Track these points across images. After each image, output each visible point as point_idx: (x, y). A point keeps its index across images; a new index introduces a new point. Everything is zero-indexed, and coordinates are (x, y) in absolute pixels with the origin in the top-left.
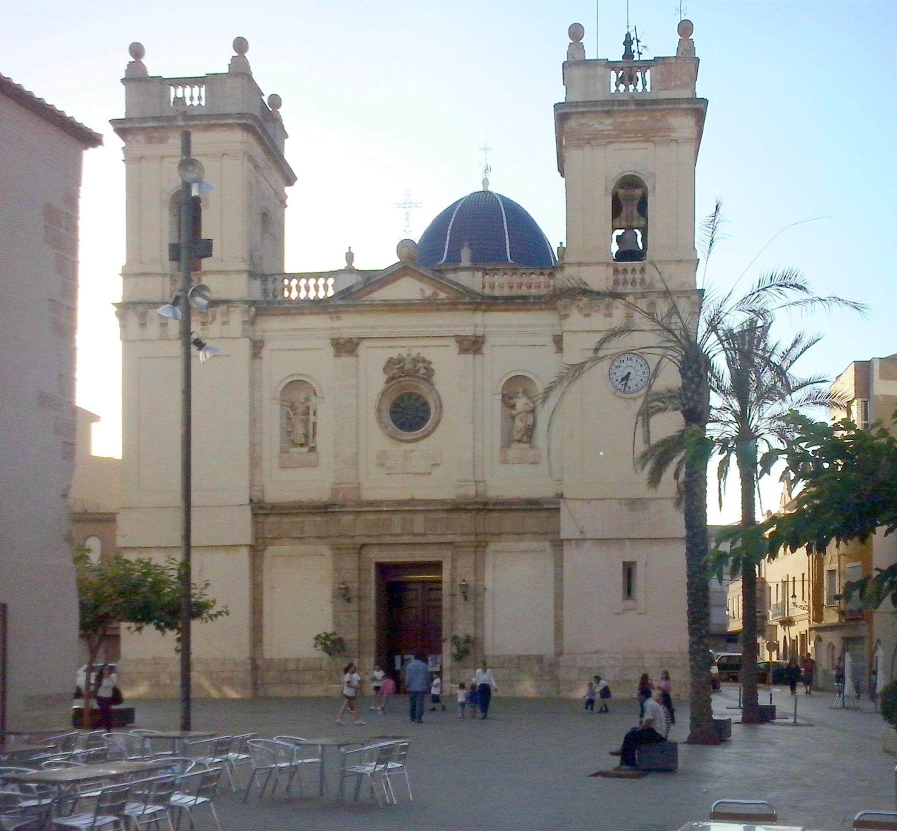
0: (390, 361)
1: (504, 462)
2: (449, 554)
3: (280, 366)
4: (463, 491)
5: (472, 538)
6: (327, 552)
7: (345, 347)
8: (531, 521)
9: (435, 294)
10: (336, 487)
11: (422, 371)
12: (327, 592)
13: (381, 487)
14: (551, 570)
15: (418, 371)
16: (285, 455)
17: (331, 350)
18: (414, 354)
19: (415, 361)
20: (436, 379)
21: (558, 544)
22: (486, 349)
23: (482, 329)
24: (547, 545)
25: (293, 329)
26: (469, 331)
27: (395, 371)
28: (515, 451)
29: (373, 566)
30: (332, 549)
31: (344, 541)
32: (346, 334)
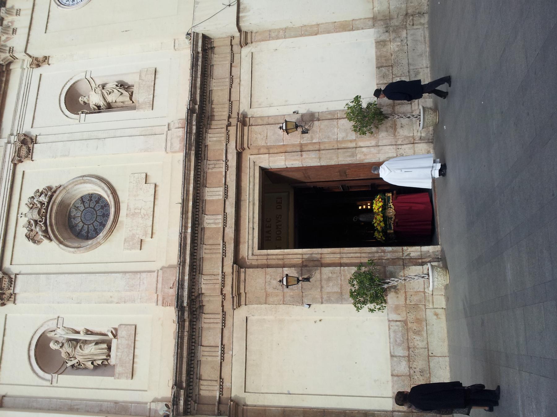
2: (252, 157)
5: (232, 130)
6: (241, 313)
10: (160, 302)
11: (43, 199)
12: (299, 312)
14: (273, 44)
15: (42, 204)
18: (24, 209)
20: (54, 185)
21: (245, 38)
23: (12, 137)
24: (246, 51)
27: (38, 229)
28: (140, 96)
29: (265, 252)
30: (239, 305)
31: (228, 289)
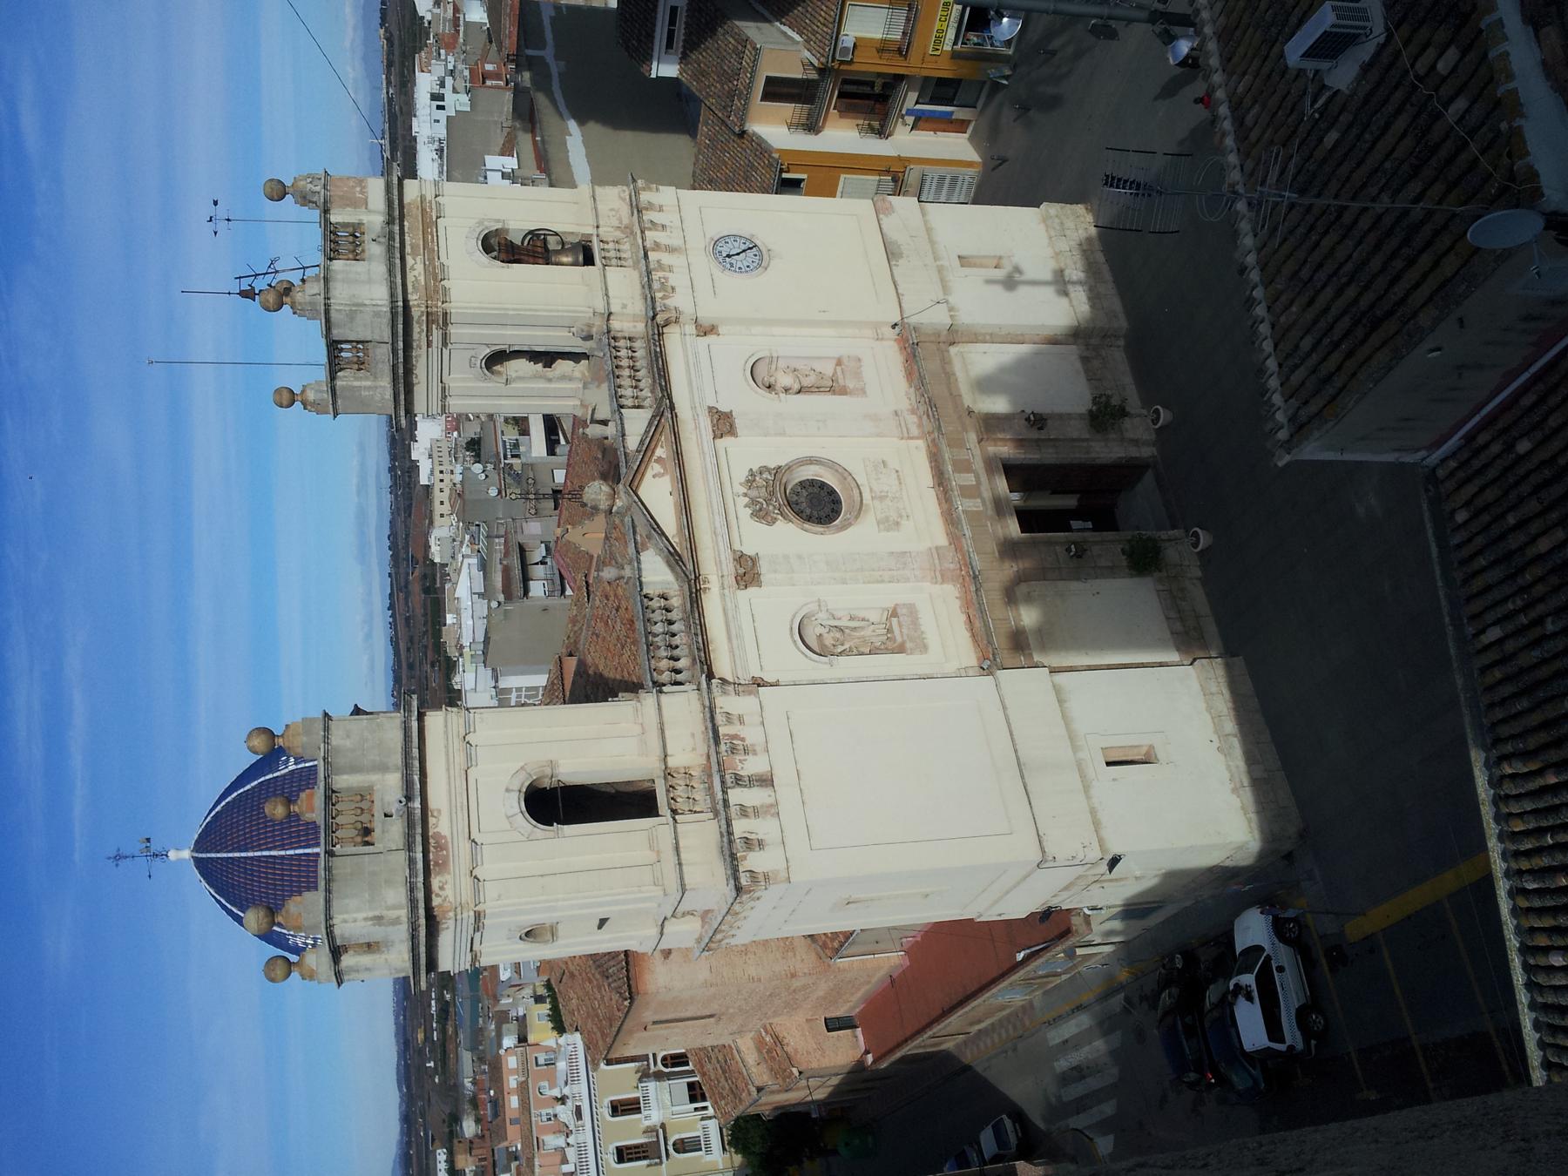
0: (760, 514)
1: (863, 392)
3: (780, 656)
4: (915, 431)
7: (747, 572)
8: (931, 366)
9: (660, 460)
13: (925, 527)
15: (767, 481)
16: (908, 645)
17: (752, 590)
19: (750, 482)
22: (724, 408)
24: (953, 350)
25: (729, 639)
26: (706, 423)
32: (729, 568)
